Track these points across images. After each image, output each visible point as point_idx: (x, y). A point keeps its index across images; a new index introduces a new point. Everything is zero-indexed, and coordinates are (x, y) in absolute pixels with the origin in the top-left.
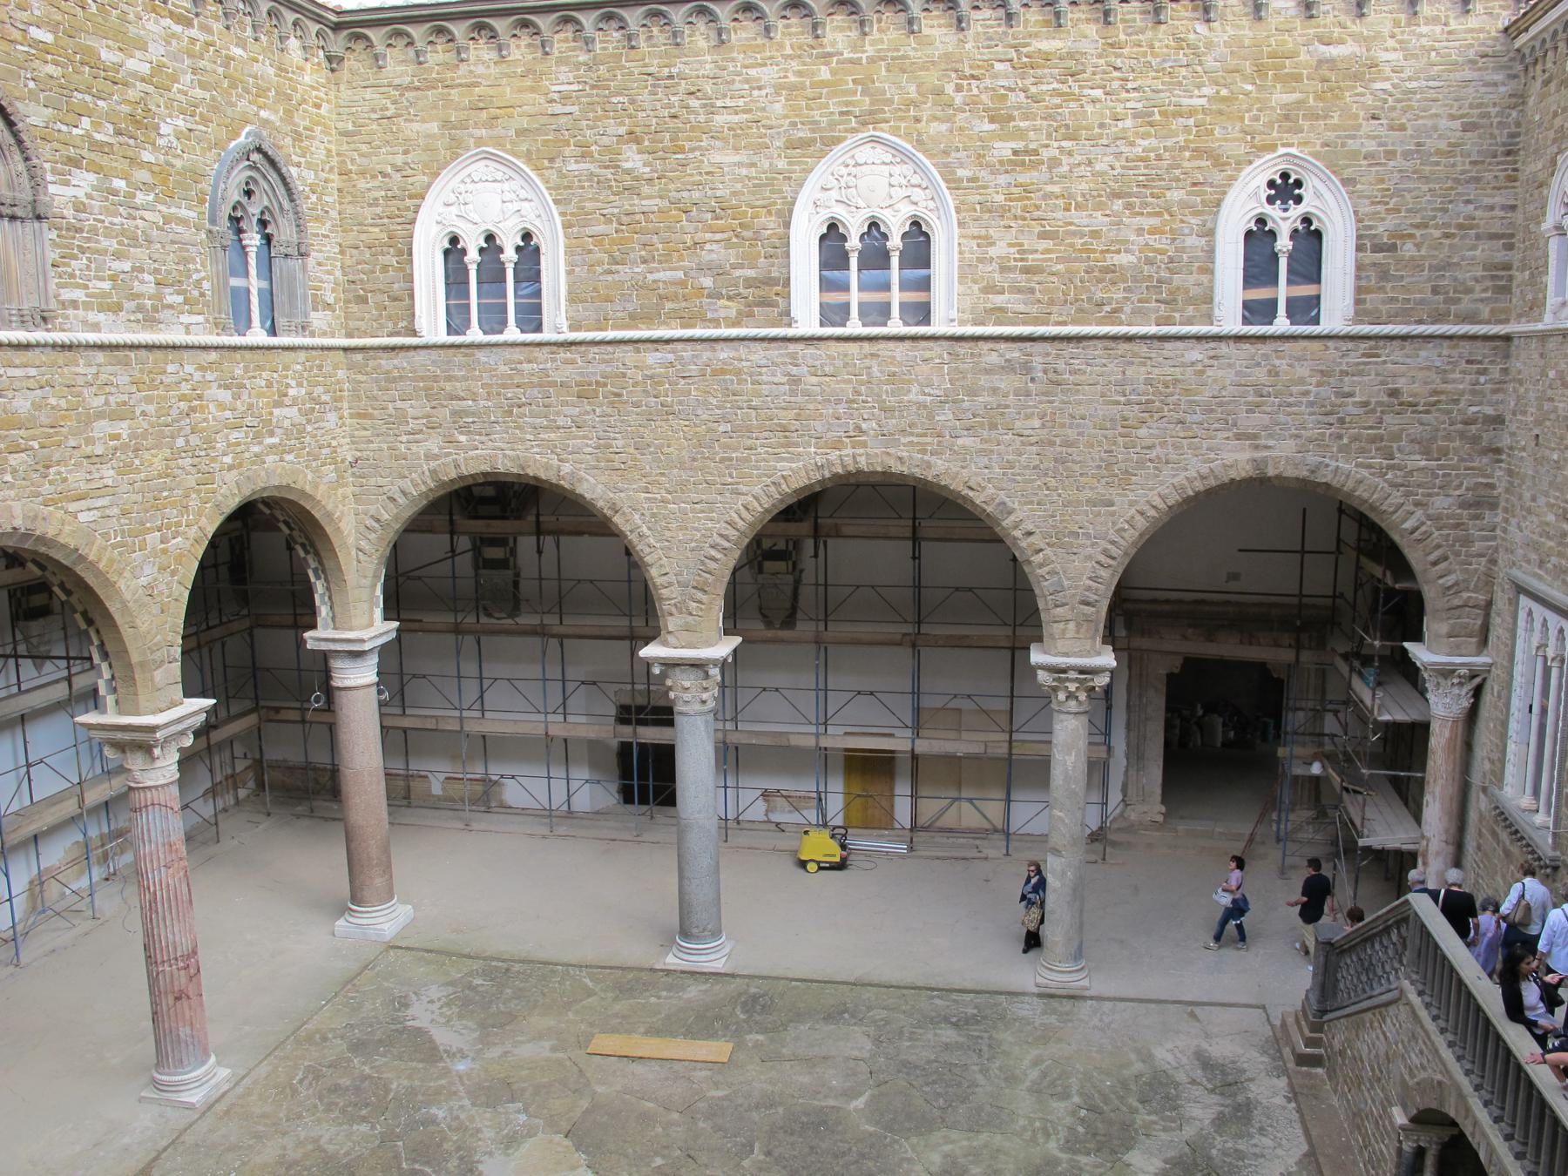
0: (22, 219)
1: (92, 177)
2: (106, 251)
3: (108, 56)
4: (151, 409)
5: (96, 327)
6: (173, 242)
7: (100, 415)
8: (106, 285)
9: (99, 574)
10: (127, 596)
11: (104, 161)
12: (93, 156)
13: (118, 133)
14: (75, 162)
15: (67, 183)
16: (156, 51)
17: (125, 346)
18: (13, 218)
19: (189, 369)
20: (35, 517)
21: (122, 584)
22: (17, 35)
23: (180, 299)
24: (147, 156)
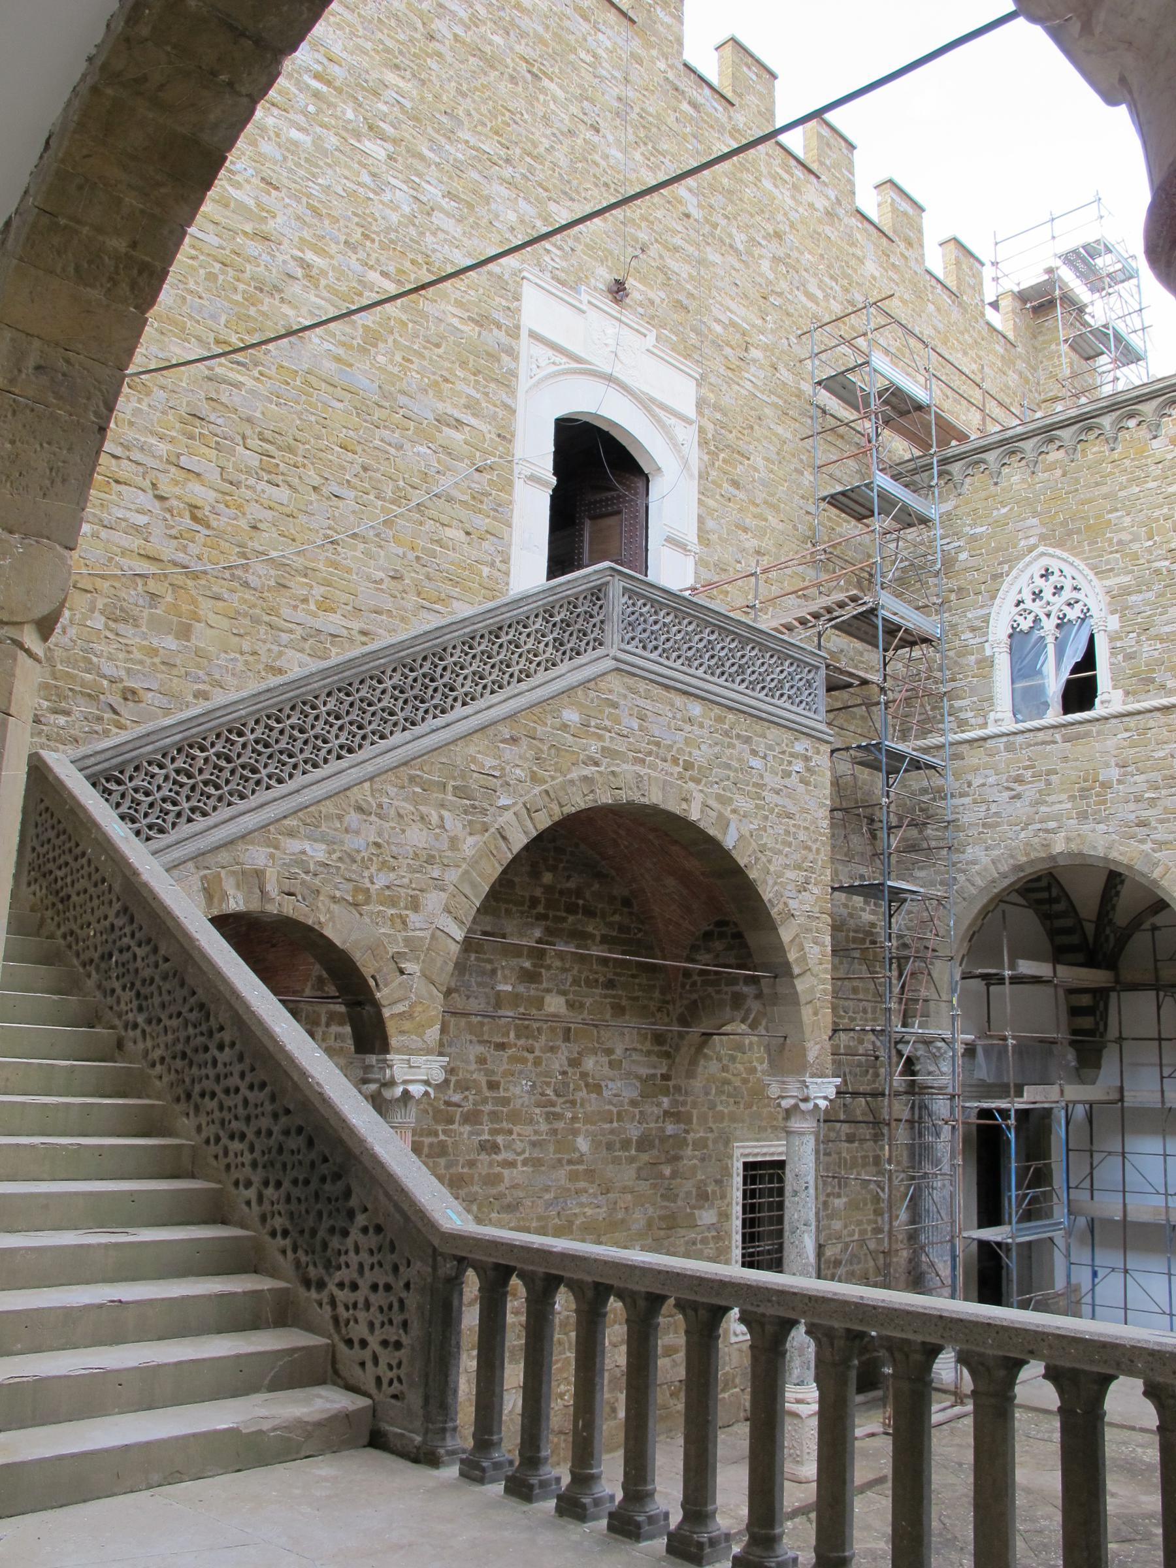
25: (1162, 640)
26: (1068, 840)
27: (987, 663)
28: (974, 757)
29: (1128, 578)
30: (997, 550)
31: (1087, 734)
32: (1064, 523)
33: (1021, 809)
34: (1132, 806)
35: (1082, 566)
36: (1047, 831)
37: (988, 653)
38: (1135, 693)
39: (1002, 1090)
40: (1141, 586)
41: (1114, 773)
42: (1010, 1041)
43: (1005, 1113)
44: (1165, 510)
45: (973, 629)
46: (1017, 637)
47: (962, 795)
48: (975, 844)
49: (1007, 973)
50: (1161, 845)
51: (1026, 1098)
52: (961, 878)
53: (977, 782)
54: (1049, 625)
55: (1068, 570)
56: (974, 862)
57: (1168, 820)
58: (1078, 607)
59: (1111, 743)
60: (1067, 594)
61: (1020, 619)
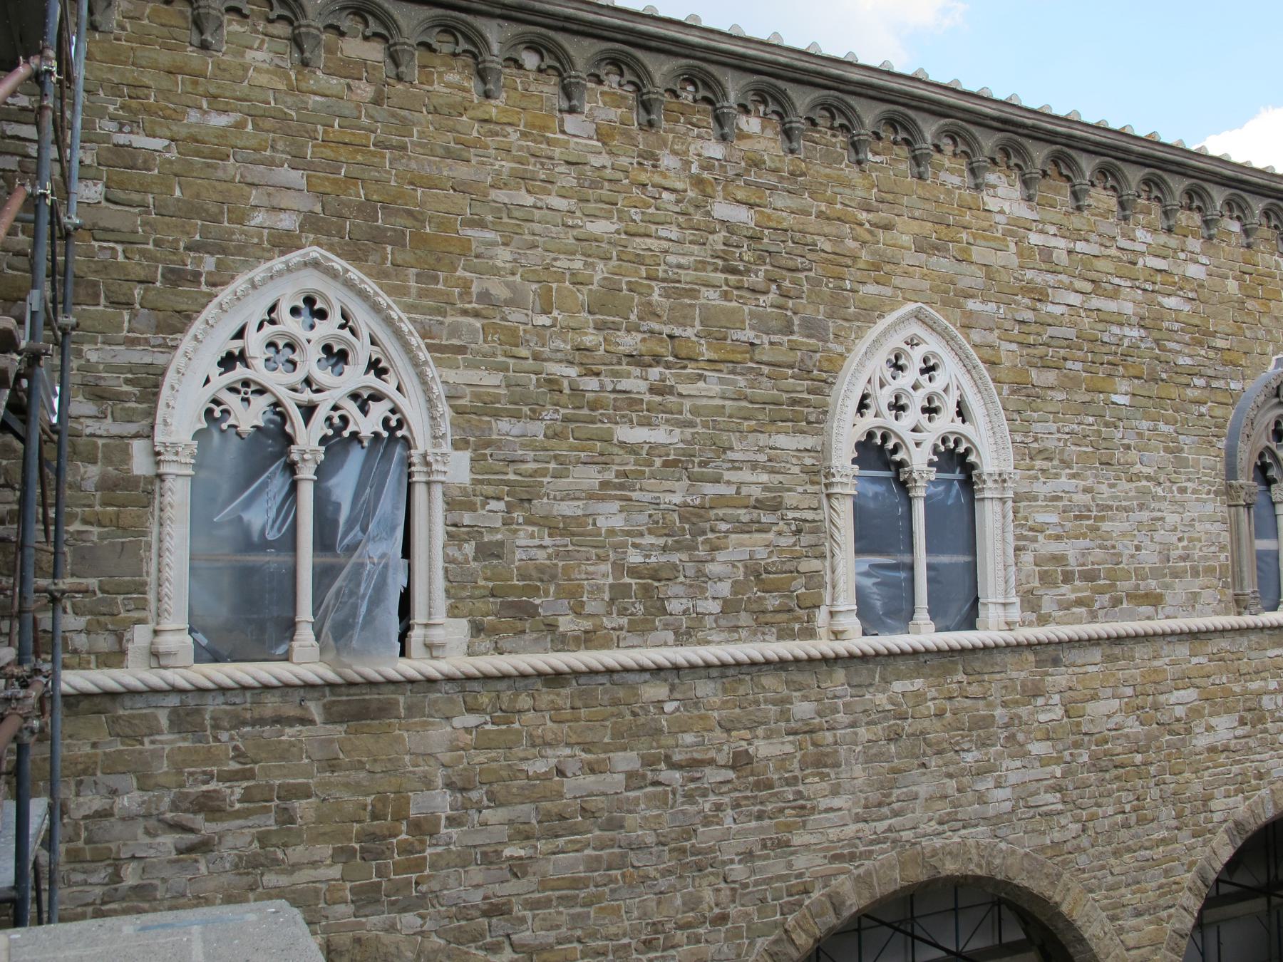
25: (553, 531)
29: (495, 379)
30: (191, 210)
31: (385, 710)
32: (367, 210)
34: (476, 874)
37: (140, 464)
38: (492, 631)
40: (521, 404)
41: (442, 802)
44: (578, 265)
45: (98, 394)
53: (92, 802)
55: (363, 318)
57: (547, 903)
58: (378, 411)
59: (439, 735)
60: (356, 376)
61: (232, 401)
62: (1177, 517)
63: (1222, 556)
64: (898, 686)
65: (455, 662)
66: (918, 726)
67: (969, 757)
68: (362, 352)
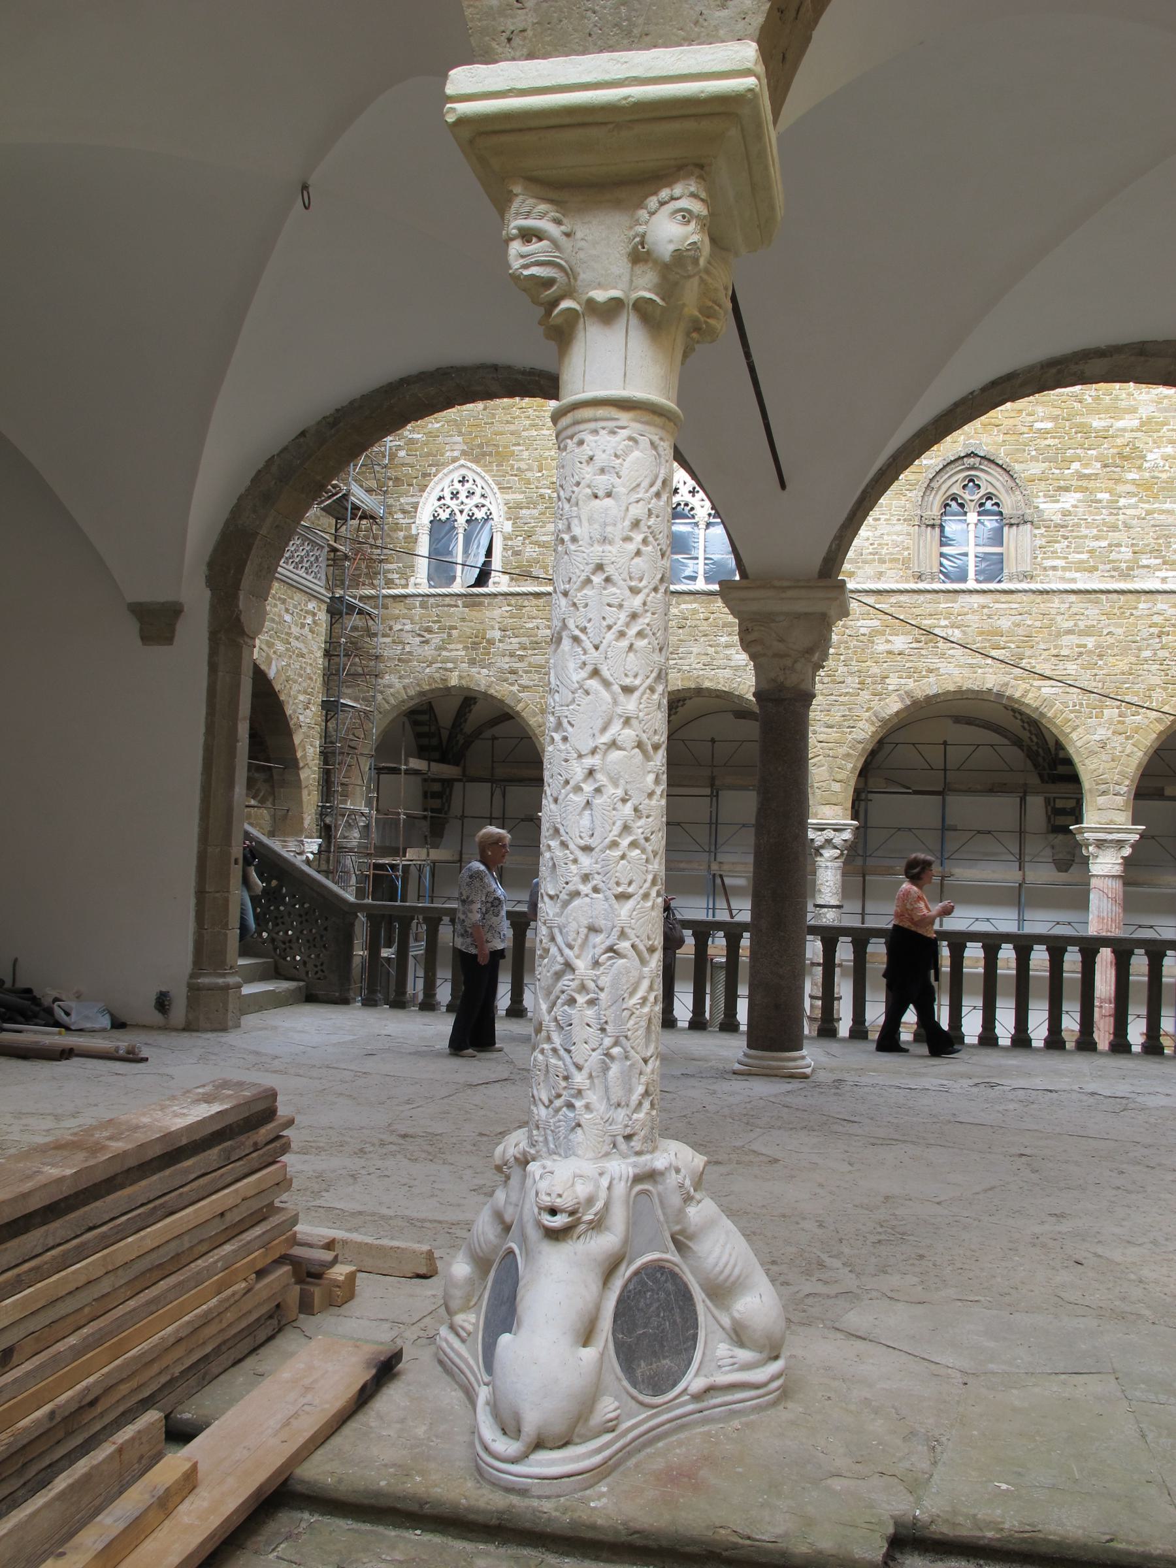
0: (1018, 525)
1: (1079, 495)
2: (1086, 537)
3: (1097, 423)
4: (1120, 631)
5: (1074, 580)
6: (1154, 526)
7: (1069, 632)
8: (1084, 556)
9: (1057, 727)
10: (1079, 744)
11: (1092, 484)
12: (1080, 483)
13: (1105, 466)
14: (1066, 489)
15: (1058, 501)
16: (1144, 412)
17: (1095, 592)
18: (1011, 525)
19: (1160, 606)
20: (1007, 684)
21: (1074, 736)
22: (1025, 429)
23: (1159, 561)
24: (1131, 476)
25: (540, 546)
26: (461, 677)
27: (414, 539)
28: (397, 609)
29: (522, 496)
30: (429, 454)
31: (480, 604)
32: (481, 446)
33: (428, 651)
34: (507, 659)
35: (490, 481)
36: (446, 670)
37: (414, 532)
39: (395, 852)
40: (531, 504)
41: (497, 634)
42: (402, 817)
43: (394, 867)
45: (404, 512)
46: (436, 523)
47: (384, 636)
48: (391, 673)
49: (403, 767)
50: (525, 688)
51: (408, 856)
52: (379, 697)
53: (397, 627)
54: (461, 520)
55: (479, 481)
56: (390, 686)
57: (530, 672)
58: (484, 510)
60: (477, 499)
62: (870, 533)
63: (906, 553)
64: (683, 606)
65: (504, 588)
66: (694, 623)
67: (723, 639)
68: (478, 491)
